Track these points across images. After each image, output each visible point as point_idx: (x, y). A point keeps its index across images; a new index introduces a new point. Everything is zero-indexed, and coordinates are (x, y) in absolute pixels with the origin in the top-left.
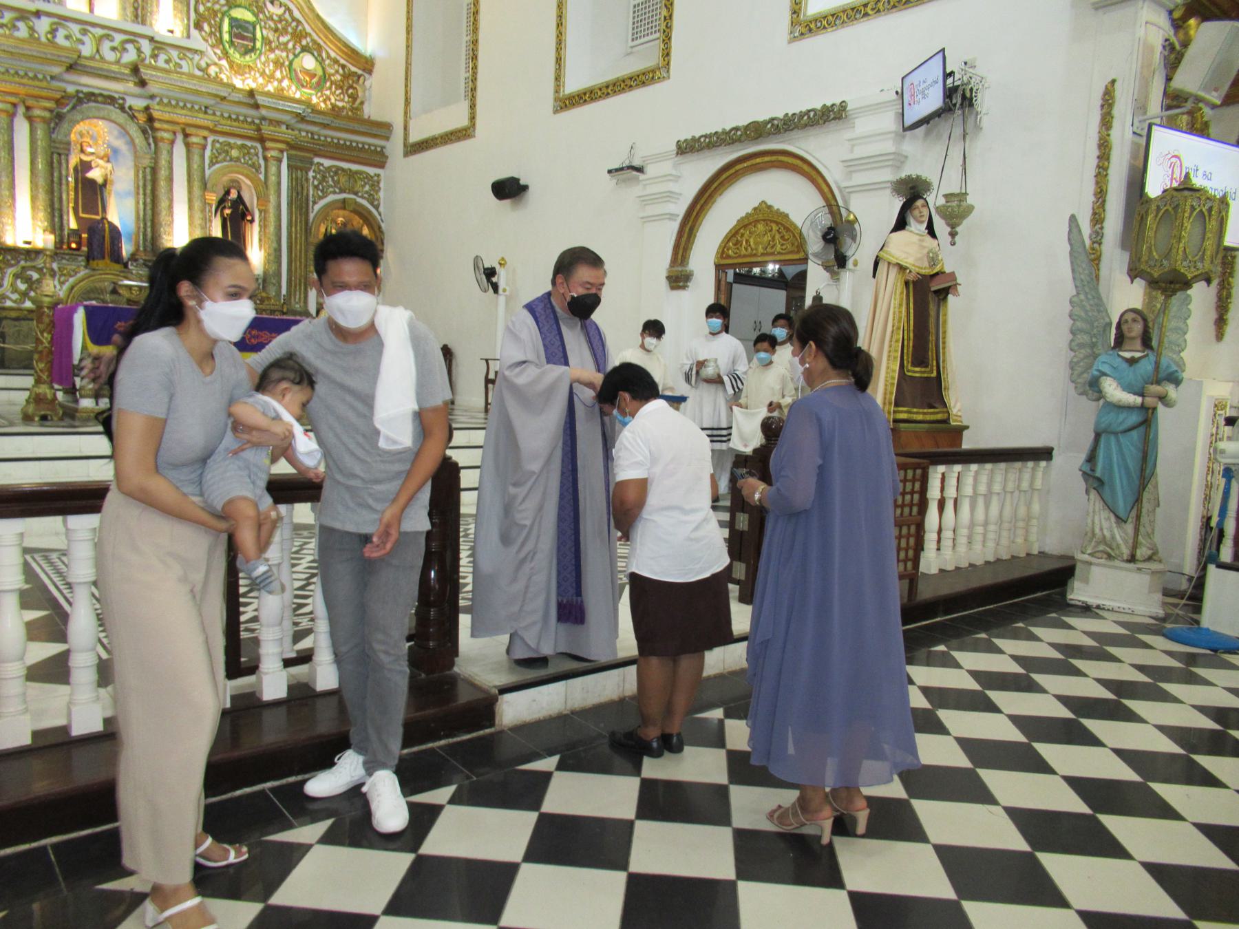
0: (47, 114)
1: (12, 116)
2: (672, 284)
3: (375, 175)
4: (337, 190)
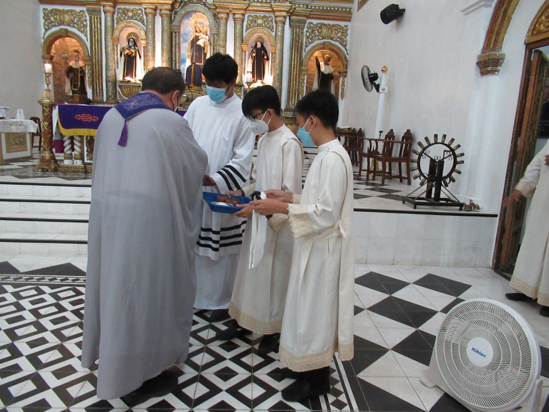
0: (168, 12)
1: (155, 15)
2: (484, 70)
3: (345, 26)
4: (321, 38)
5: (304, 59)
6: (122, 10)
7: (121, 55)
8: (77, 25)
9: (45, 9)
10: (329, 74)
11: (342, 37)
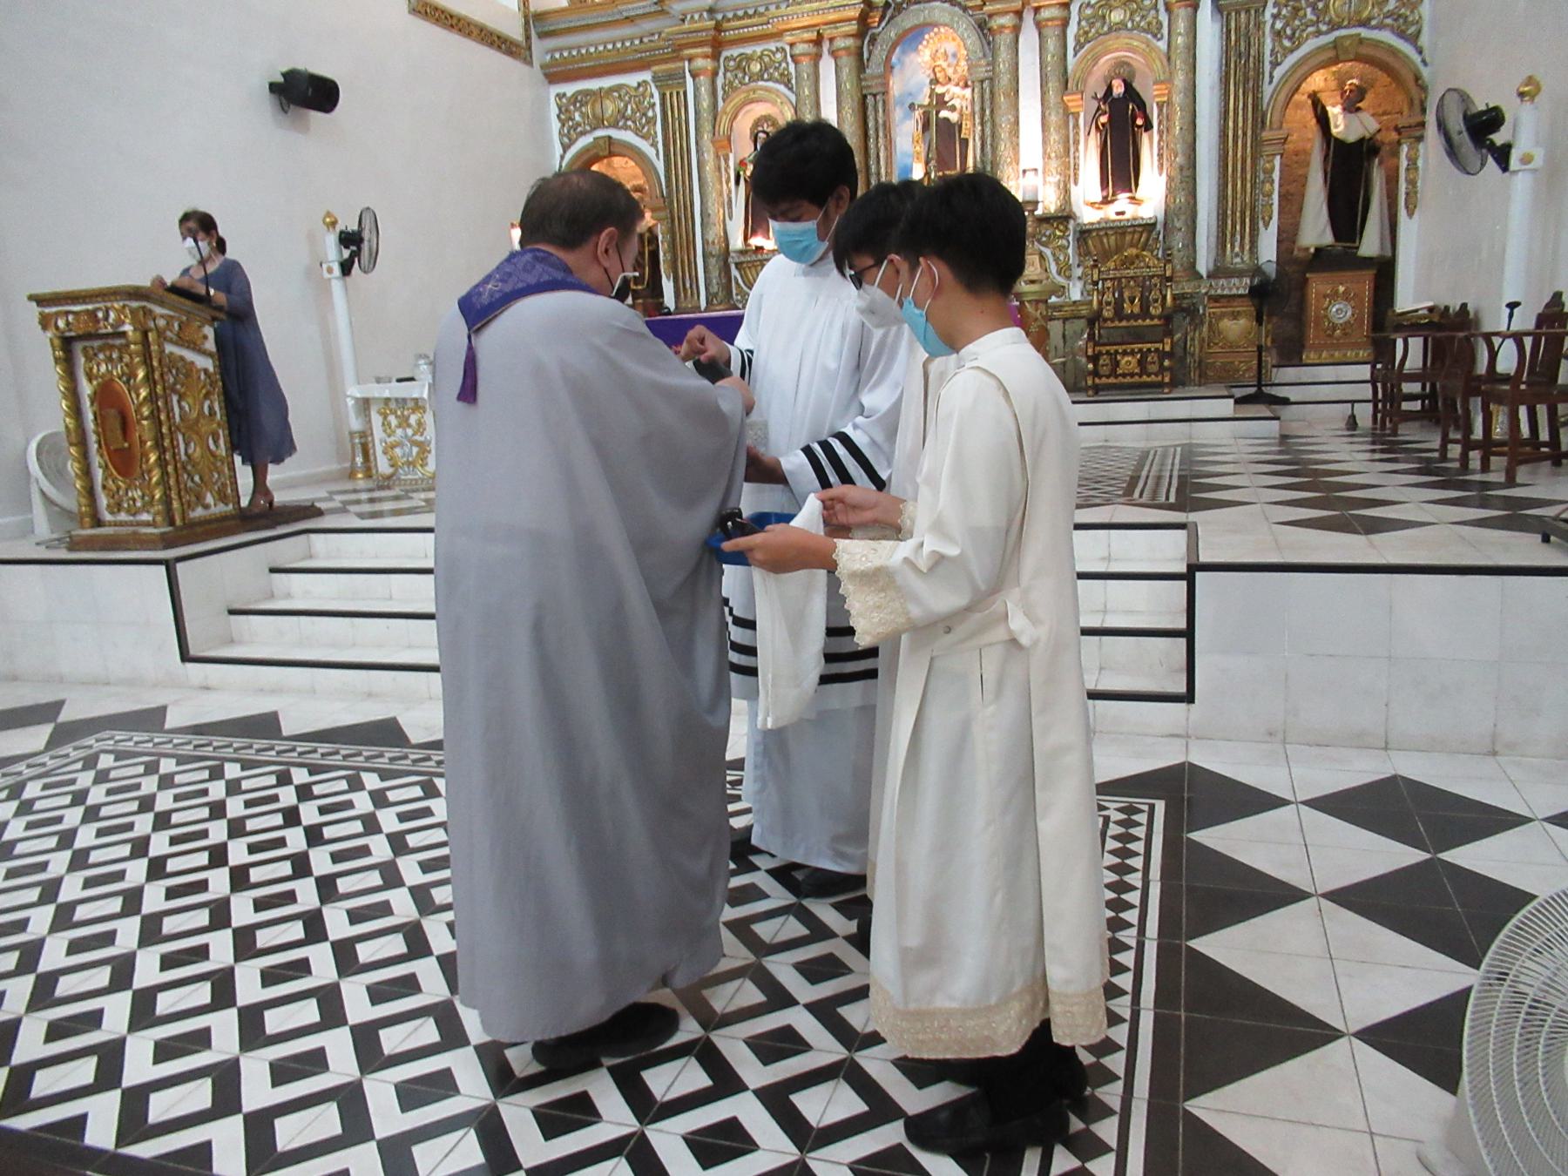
0: (850, 42)
1: (817, 57)
4: (1324, 28)
5: (1268, 104)
6: (735, 60)
7: (737, 182)
8: (634, 122)
9: (560, 96)
10: (1362, 140)
11: (1403, 11)
